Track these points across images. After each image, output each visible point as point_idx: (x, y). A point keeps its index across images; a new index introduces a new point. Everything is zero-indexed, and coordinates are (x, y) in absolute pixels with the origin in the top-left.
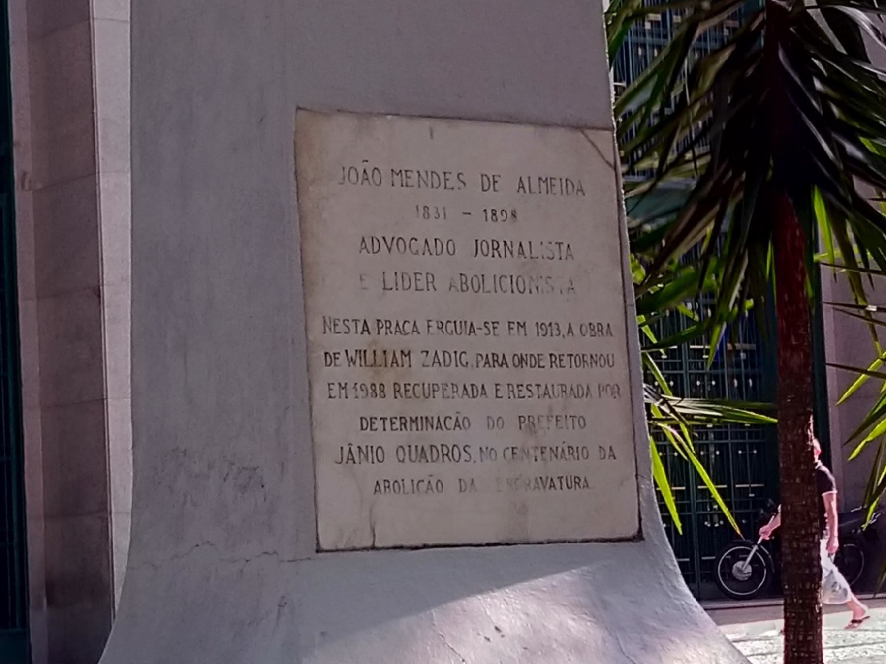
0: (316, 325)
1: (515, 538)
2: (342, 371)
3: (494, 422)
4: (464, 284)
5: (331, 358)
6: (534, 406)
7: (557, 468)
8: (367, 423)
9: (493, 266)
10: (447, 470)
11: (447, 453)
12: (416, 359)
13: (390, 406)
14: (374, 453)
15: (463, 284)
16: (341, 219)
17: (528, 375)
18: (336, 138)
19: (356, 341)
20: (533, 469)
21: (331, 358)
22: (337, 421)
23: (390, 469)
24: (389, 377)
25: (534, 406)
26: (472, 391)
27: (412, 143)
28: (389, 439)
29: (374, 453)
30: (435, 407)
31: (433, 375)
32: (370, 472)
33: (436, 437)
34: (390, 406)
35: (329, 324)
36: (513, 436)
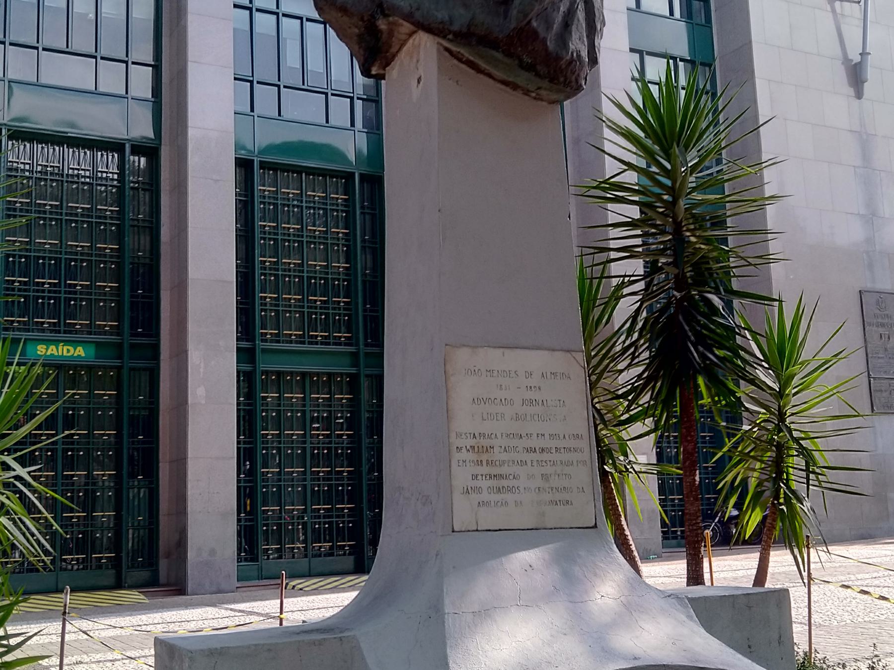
0: (453, 435)
1: (539, 526)
2: (464, 455)
3: (531, 477)
4: (517, 417)
5: (459, 449)
6: (549, 470)
7: (558, 496)
8: (475, 477)
9: (531, 410)
10: (508, 497)
11: (510, 490)
12: (496, 450)
13: (485, 470)
14: (479, 490)
15: (517, 417)
16: (465, 390)
17: (545, 456)
18: (462, 356)
19: (470, 442)
20: (548, 497)
21: (459, 449)
22: (461, 477)
23: (485, 496)
24: (484, 457)
25: (549, 470)
26: (523, 463)
27: (494, 358)
28: (485, 484)
29: (479, 490)
30: (504, 470)
31: (504, 456)
32: (474, 496)
33: (505, 483)
34: (485, 470)
35: (459, 435)
36: (539, 482)
